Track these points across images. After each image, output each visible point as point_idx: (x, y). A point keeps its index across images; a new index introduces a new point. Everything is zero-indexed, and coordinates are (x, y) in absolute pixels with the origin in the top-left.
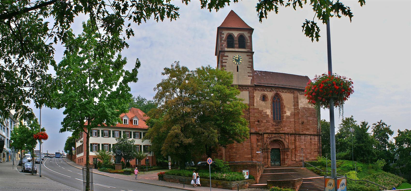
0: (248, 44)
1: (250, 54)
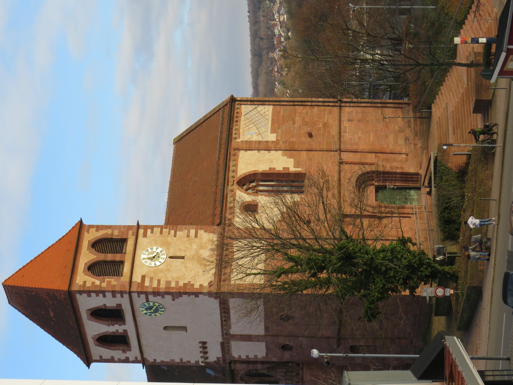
1: (141, 231)
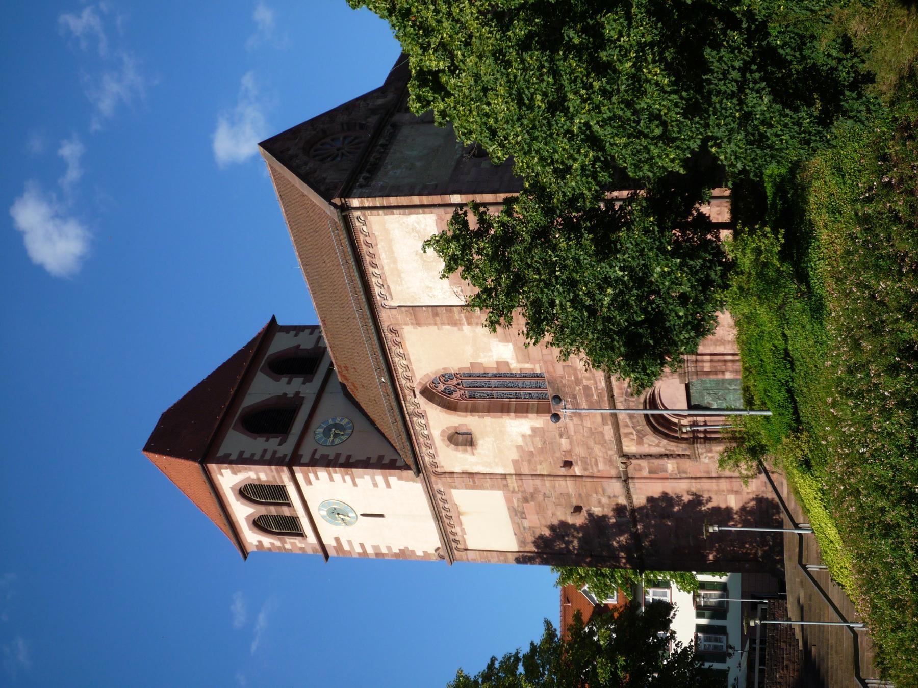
0: (263, 477)
1: (300, 477)
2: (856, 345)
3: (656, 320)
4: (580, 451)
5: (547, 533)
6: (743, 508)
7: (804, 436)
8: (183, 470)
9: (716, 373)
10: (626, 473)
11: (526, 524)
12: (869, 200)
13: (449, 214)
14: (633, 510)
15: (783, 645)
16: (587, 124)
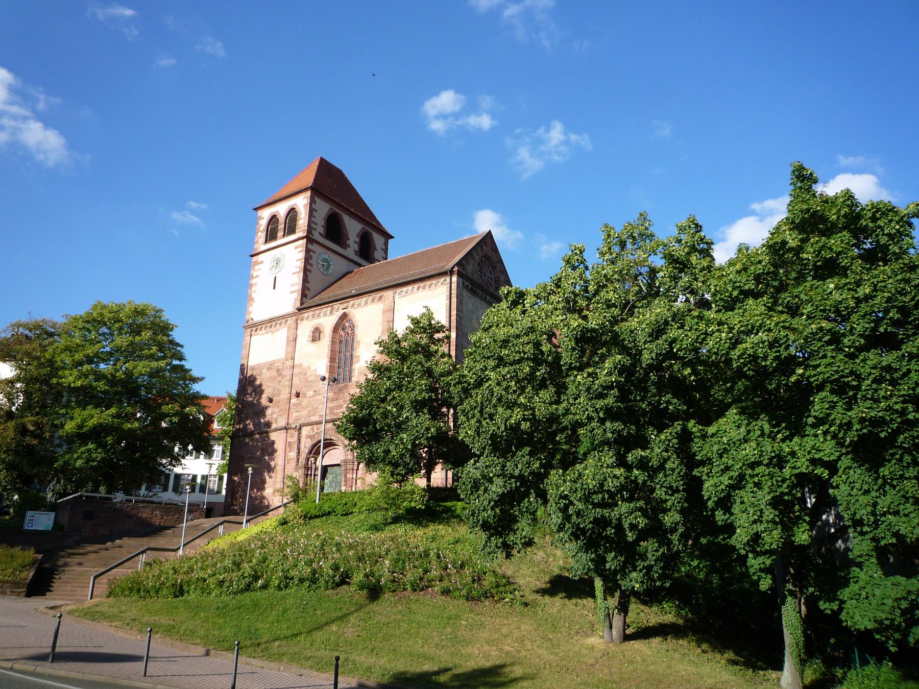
2: (351, 547)
3: (376, 436)
4: (304, 401)
5: (258, 383)
6: (264, 498)
7: (301, 521)
8: (308, 178)
9: (345, 481)
10: (290, 428)
11: (264, 371)
12: (439, 557)
13: (444, 322)
14: (267, 433)
15: (176, 516)
16: (490, 379)
